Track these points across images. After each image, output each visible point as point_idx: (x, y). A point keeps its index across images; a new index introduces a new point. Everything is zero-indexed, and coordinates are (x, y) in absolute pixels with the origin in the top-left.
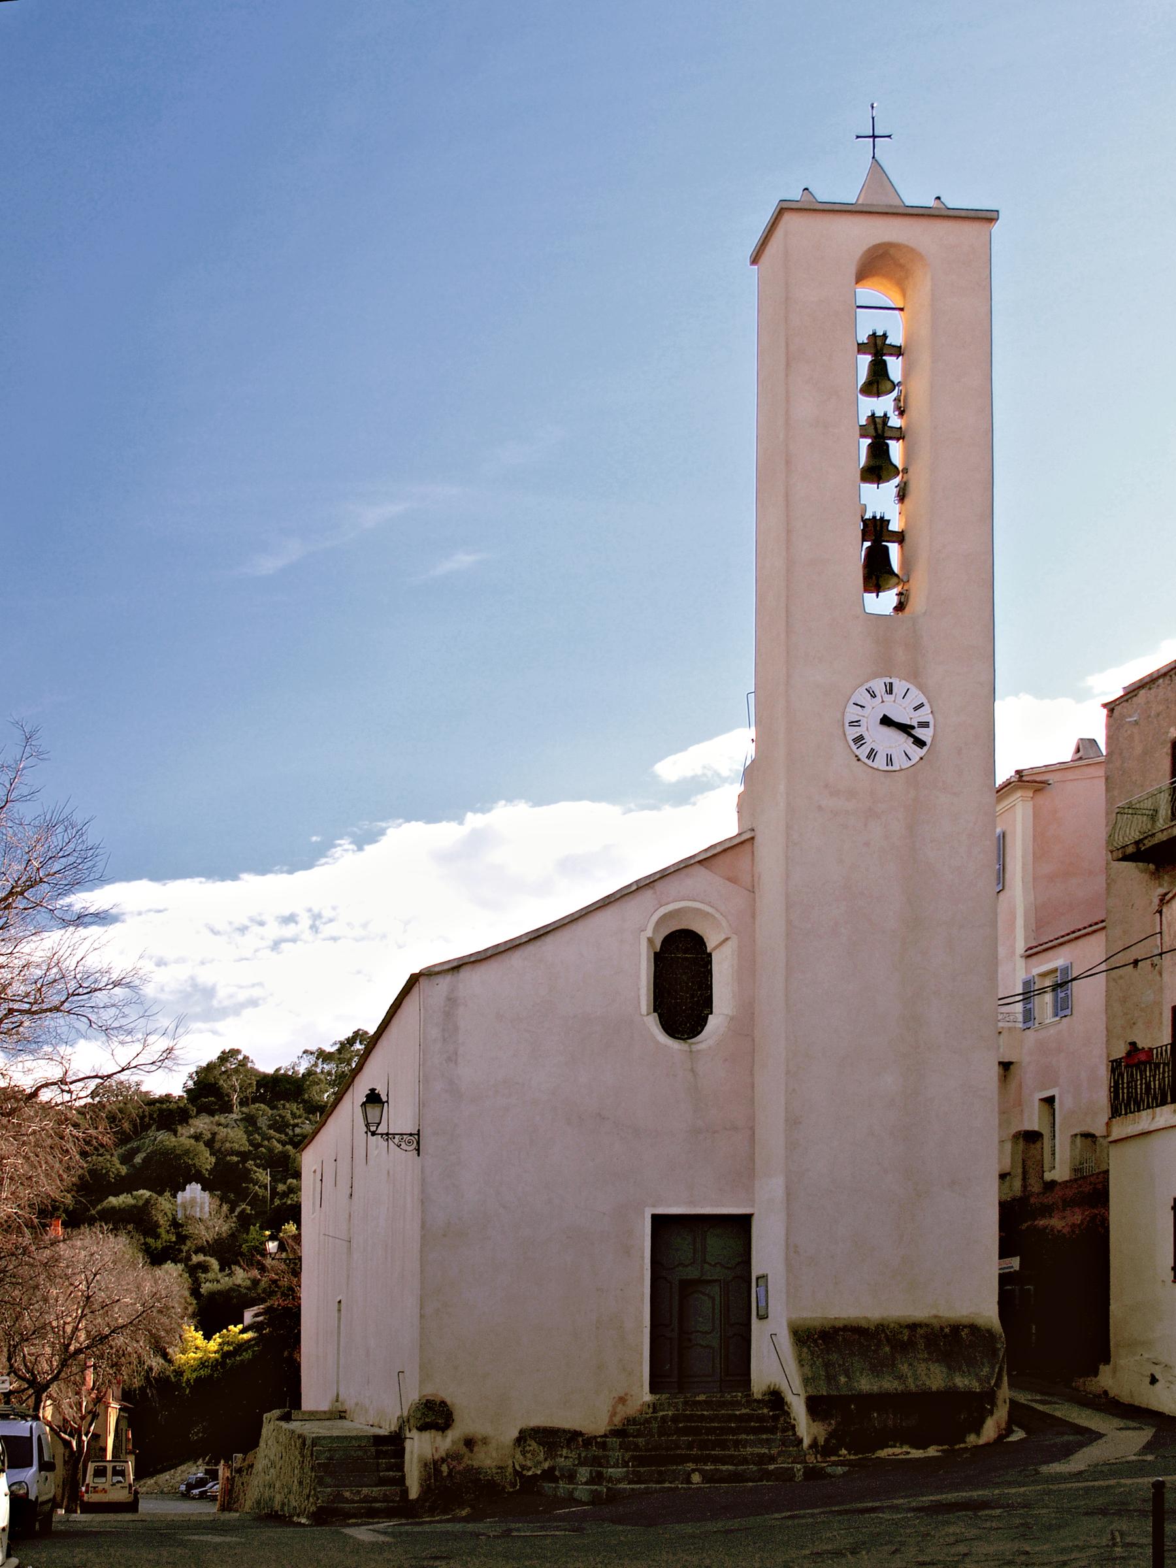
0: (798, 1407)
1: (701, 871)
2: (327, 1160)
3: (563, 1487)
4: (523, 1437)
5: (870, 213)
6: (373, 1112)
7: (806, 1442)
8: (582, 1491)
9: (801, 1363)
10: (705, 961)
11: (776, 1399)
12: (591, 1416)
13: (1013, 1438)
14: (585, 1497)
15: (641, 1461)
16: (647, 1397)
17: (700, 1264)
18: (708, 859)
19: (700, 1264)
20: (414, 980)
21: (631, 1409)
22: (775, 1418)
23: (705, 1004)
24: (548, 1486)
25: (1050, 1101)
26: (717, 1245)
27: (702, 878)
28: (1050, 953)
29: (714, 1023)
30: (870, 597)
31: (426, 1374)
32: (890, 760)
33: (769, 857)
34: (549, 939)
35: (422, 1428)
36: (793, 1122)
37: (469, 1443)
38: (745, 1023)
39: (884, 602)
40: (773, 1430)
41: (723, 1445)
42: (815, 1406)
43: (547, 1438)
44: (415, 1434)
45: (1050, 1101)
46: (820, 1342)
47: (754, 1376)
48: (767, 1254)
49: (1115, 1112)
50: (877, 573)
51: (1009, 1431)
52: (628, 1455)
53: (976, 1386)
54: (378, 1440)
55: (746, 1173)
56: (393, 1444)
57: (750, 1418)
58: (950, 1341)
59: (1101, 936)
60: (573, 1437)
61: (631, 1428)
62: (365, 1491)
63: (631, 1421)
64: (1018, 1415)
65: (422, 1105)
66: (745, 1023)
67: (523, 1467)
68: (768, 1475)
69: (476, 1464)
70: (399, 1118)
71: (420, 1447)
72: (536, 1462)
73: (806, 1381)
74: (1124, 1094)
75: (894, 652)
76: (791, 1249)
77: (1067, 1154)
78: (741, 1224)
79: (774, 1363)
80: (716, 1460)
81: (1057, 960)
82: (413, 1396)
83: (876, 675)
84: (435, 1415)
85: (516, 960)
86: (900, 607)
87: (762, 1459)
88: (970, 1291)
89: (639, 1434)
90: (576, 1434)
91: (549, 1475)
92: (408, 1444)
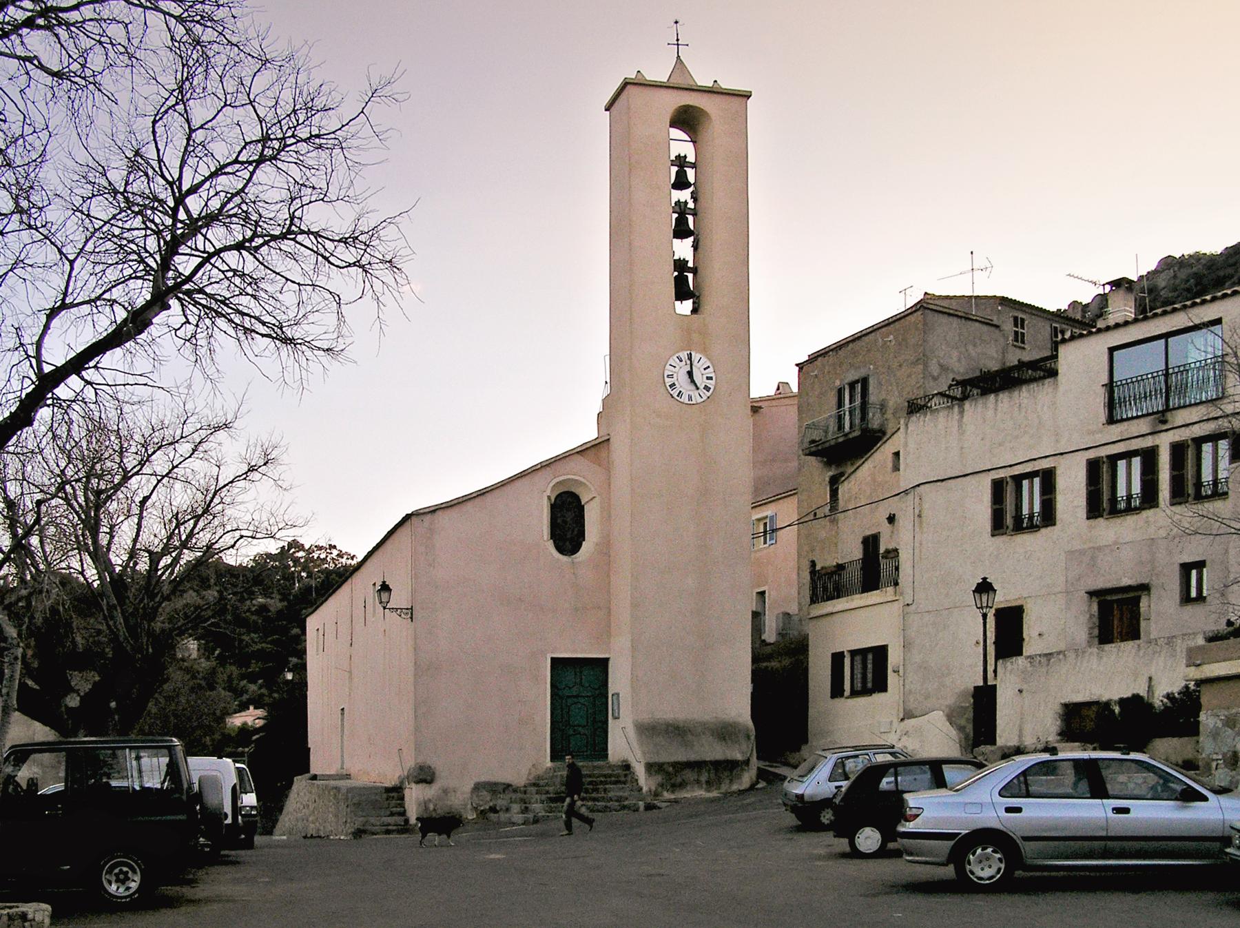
0: (640, 770)
1: (578, 457)
2: (320, 625)
3: (503, 816)
4: (478, 787)
5: (888, 324)
6: (385, 596)
7: (645, 789)
8: (518, 818)
9: (641, 744)
10: (580, 509)
11: (627, 767)
12: (517, 774)
13: (759, 786)
14: (520, 822)
15: (552, 800)
16: (549, 764)
17: (580, 689)
18: (584, 451)
19: (580, 689)
20: (408, 517)
21: (540, 772)
22: (626, 776)
23: (581, 536)
24: (492, 816)
25: (762, 594)
26: (588, 675)
27: (580, 463)
28: (763, 508)
29: (586, 546)
30: (678, 303)
31: (418, 748)
32: (690, 398)
33: (620, 451)
34: (488, 497)
35: (417, 782)
36: (635, 605)
37: (445, 791)
38: (606, 546)
39: (686, 307)
40: (625, 783)
41: (597, 790)
42: (651, 768)
43: (495, 788)
44: (413, 785)
45: (762, 594)
46: (648, 730)
47: (610, 752)
48: (618, 681)
49: (814, 600)
50: (682, 292)
51: (757, 783)
52: (544, 797)
53: (739, 757)
54: (388, 790)
55: (605, 632)
56: (396, 792)
57: (610, 776)
58: (725, 732)
59: (794, 499)
60: (507, 787)
61: (542, 783)
62: (384, 819)
63: (538, 778)
64: (762, 774)
65: (414, 592)
66: (606, 546)
67: (479, 805)
68: (624, 807)
69: (449, 803)
70: (399, 598)
71: (414, 797)
72: (486, 800)
73: (644, 753)
74: (820, 591)
75: (691, 339)
76: (635, 680)
77: (774, 625)
78: (603, 664)
79: (623, 743)
80: (594, 799)
81: (768, 511)
82: (410, 763)
83: (683, 350)
84: (425, 776)
85: (469, 506)
86: (695, 310)
87: (619, 799)
88: (737, 704)
89: (547, 785)
90: (509, 785)
91: (493, 810)
92: (407, 792)
